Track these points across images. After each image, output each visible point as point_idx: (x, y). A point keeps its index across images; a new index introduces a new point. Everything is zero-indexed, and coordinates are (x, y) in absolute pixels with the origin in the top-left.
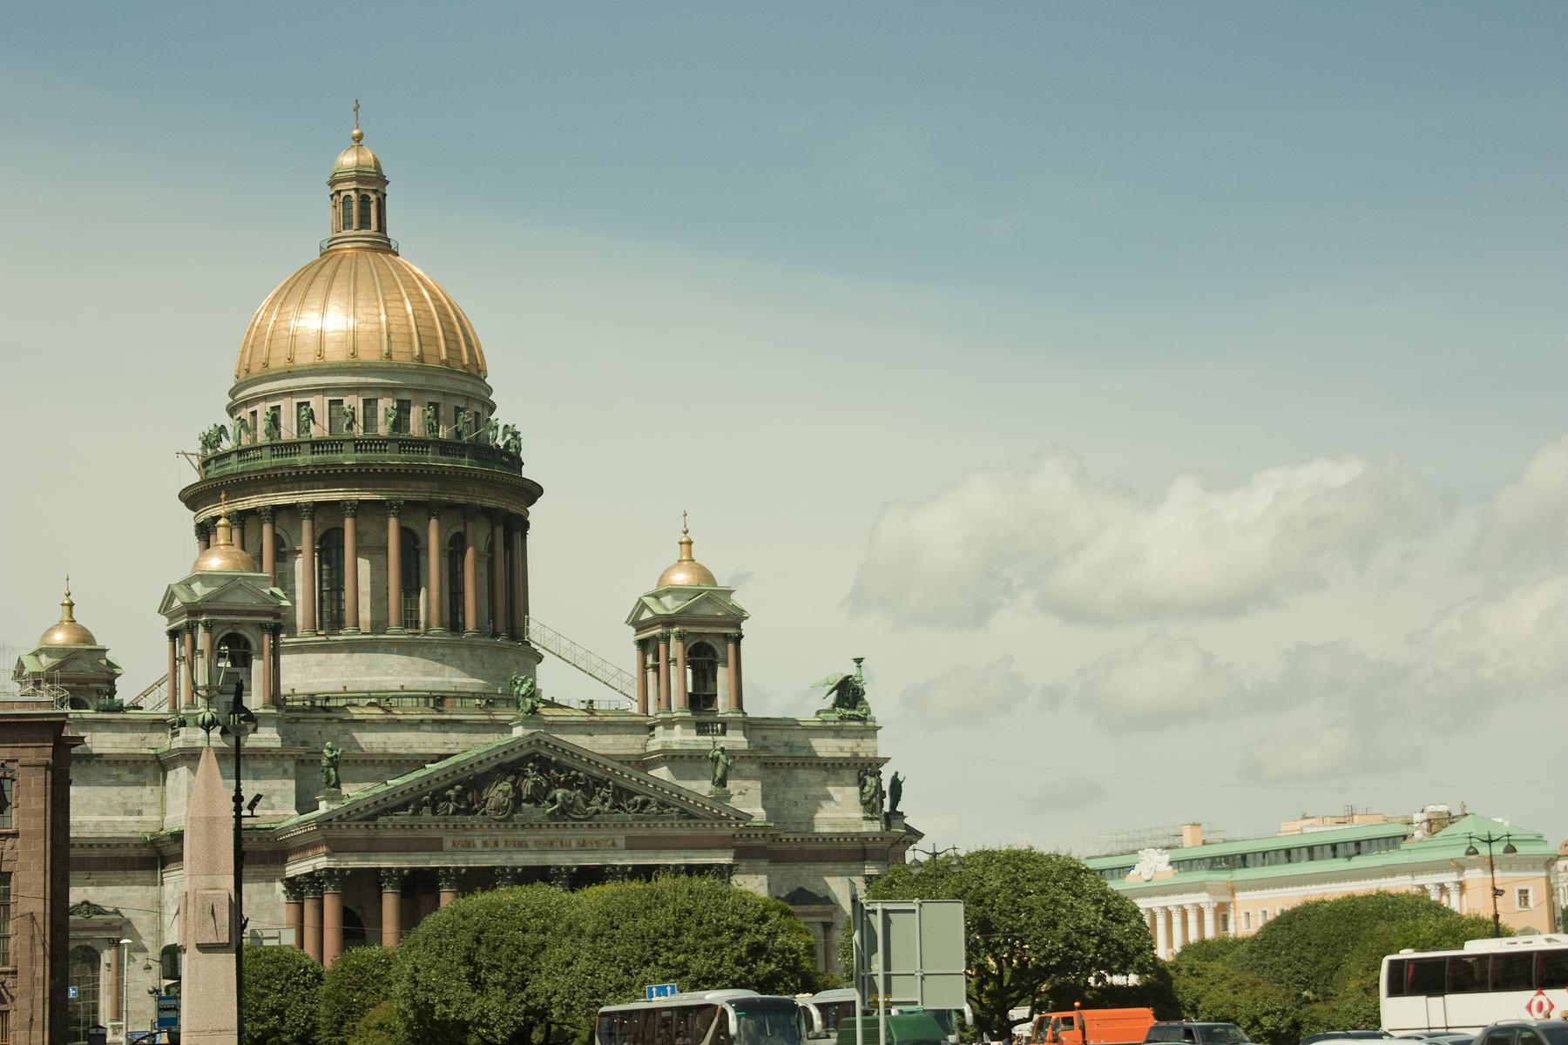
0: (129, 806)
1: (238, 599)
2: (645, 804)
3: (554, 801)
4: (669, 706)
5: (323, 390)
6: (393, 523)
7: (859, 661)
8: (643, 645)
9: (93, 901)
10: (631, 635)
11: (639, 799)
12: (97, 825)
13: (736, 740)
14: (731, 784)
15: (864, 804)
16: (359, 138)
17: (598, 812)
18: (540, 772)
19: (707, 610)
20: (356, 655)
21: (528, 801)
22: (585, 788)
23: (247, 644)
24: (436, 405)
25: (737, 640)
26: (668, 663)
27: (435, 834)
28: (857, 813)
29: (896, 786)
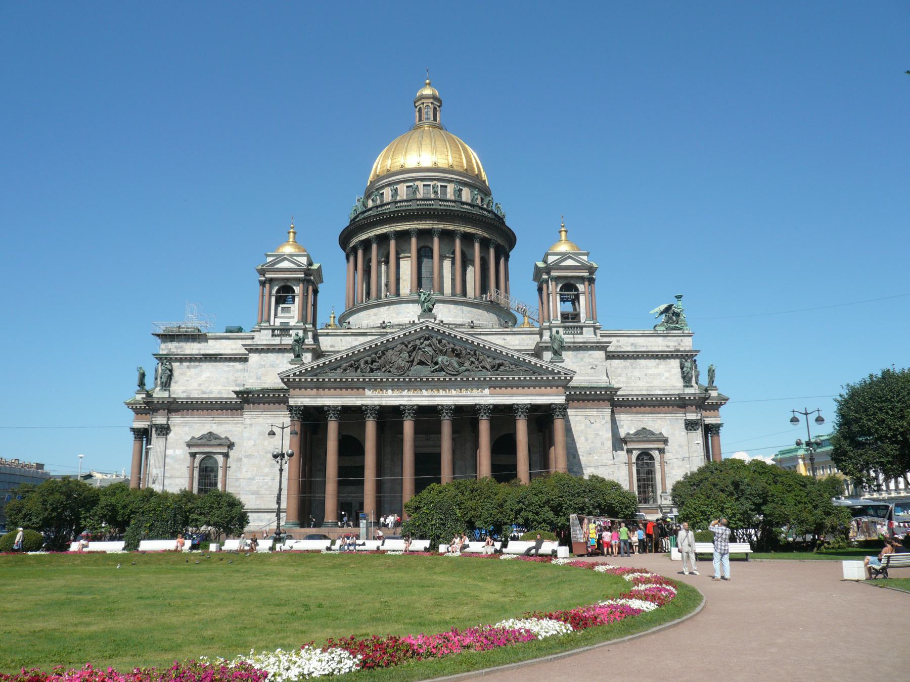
0: (239, 382)
1: (285, 264)
2: (500, 365)
3: (436, 363)
4: (549, 319)
5: (389, 185)
6: (414, 241)
7: (679, 297)
8: (540, 290)
9: (215, 432)
10: (535, 285)
11: (497, 362)
12: (220, 392)
13: (588, 335)
14: (565, 354)
15: (684, 378)
16: (429, 84)
17: (467, 370)
18: (430, 345)
19: (569, 262)
20: (392, 307)
21: (421, 363)
22: (458, 355)
23: (294, 292)
24: (446, 187)
25: (591, 281)
26: (548, 294)
27: (359, 385)
28: (680, 383)
29: (711, 373)
